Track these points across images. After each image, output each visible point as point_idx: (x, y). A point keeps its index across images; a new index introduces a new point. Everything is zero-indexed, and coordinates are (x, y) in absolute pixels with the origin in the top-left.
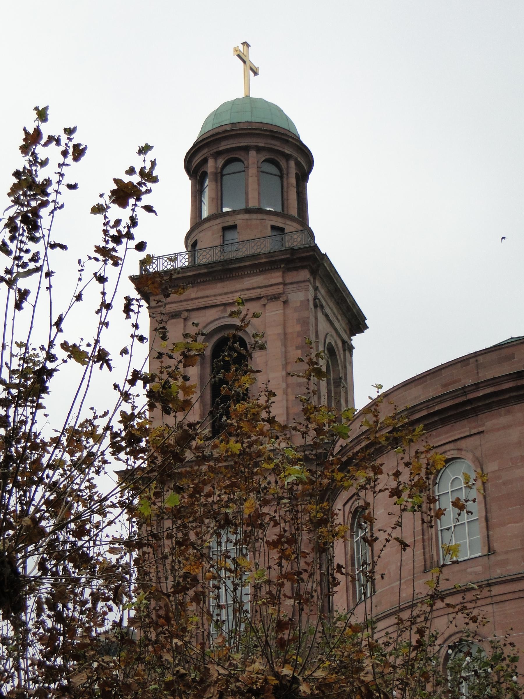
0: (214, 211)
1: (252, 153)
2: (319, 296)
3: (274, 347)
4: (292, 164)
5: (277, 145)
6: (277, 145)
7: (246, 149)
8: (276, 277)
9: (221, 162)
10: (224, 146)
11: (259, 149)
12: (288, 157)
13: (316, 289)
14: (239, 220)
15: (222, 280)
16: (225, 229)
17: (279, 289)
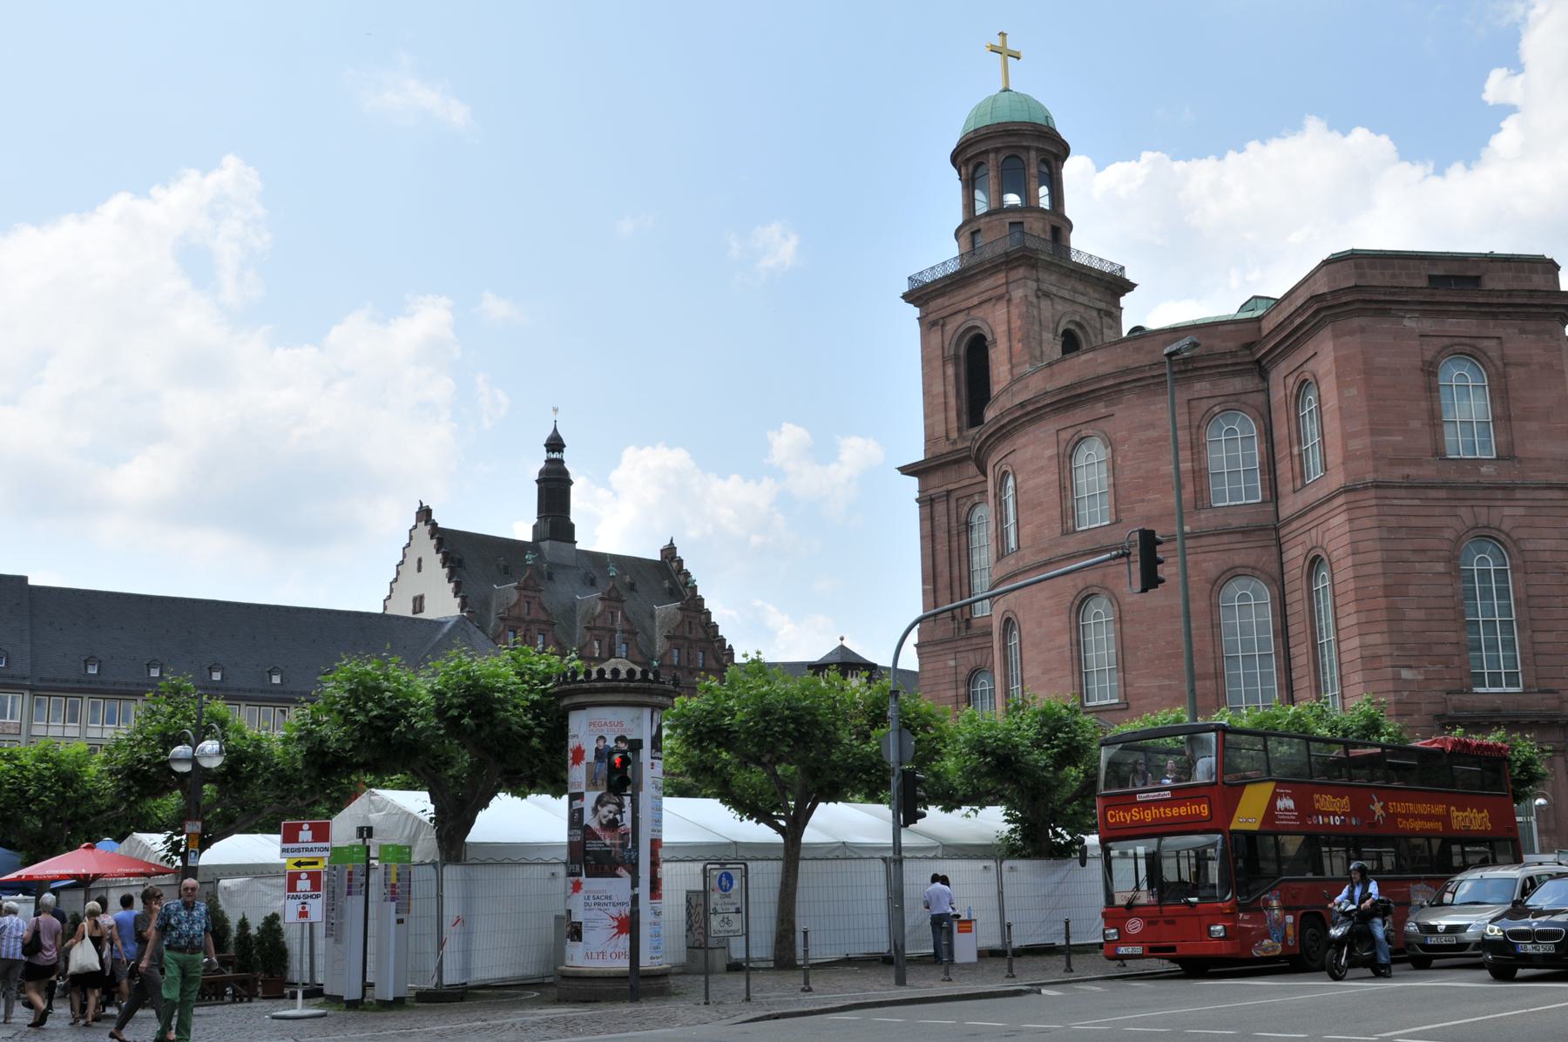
0: (994, 205)
1: (992, 156)
2: (1045, 287)
3: (1002, 344)
4: (1033, 154)
5: (1013, 141)
6: (1013, 141)
7: (986, 152)
8: (1000, 278)
9: (971, 168)
10: (970, 152)
11: (997, 150)
12: (1028, 148)
13: (1038, 280)
14: (982, 224)
15: (964, 287)
16: (973, 234)
17: (1003, 290)
